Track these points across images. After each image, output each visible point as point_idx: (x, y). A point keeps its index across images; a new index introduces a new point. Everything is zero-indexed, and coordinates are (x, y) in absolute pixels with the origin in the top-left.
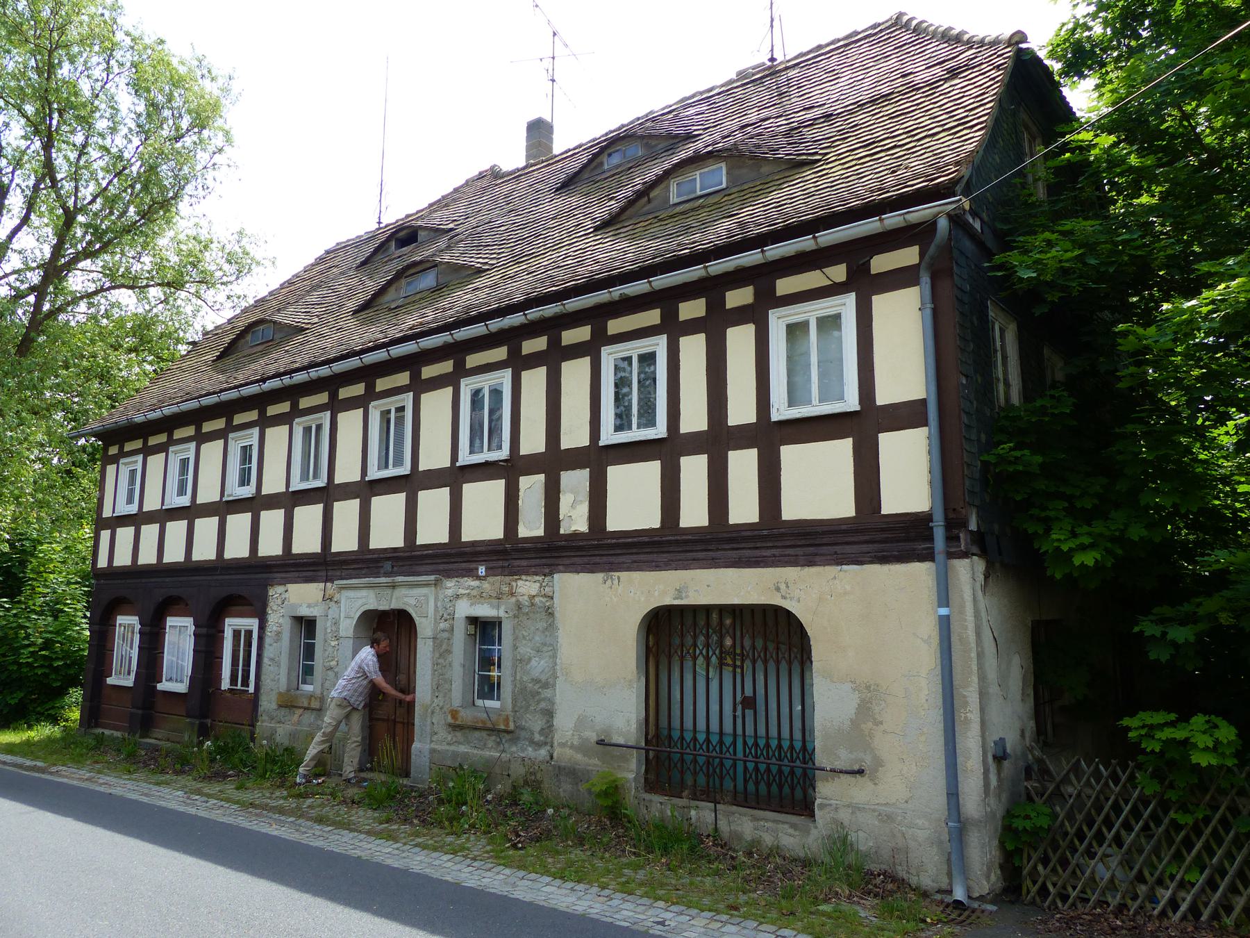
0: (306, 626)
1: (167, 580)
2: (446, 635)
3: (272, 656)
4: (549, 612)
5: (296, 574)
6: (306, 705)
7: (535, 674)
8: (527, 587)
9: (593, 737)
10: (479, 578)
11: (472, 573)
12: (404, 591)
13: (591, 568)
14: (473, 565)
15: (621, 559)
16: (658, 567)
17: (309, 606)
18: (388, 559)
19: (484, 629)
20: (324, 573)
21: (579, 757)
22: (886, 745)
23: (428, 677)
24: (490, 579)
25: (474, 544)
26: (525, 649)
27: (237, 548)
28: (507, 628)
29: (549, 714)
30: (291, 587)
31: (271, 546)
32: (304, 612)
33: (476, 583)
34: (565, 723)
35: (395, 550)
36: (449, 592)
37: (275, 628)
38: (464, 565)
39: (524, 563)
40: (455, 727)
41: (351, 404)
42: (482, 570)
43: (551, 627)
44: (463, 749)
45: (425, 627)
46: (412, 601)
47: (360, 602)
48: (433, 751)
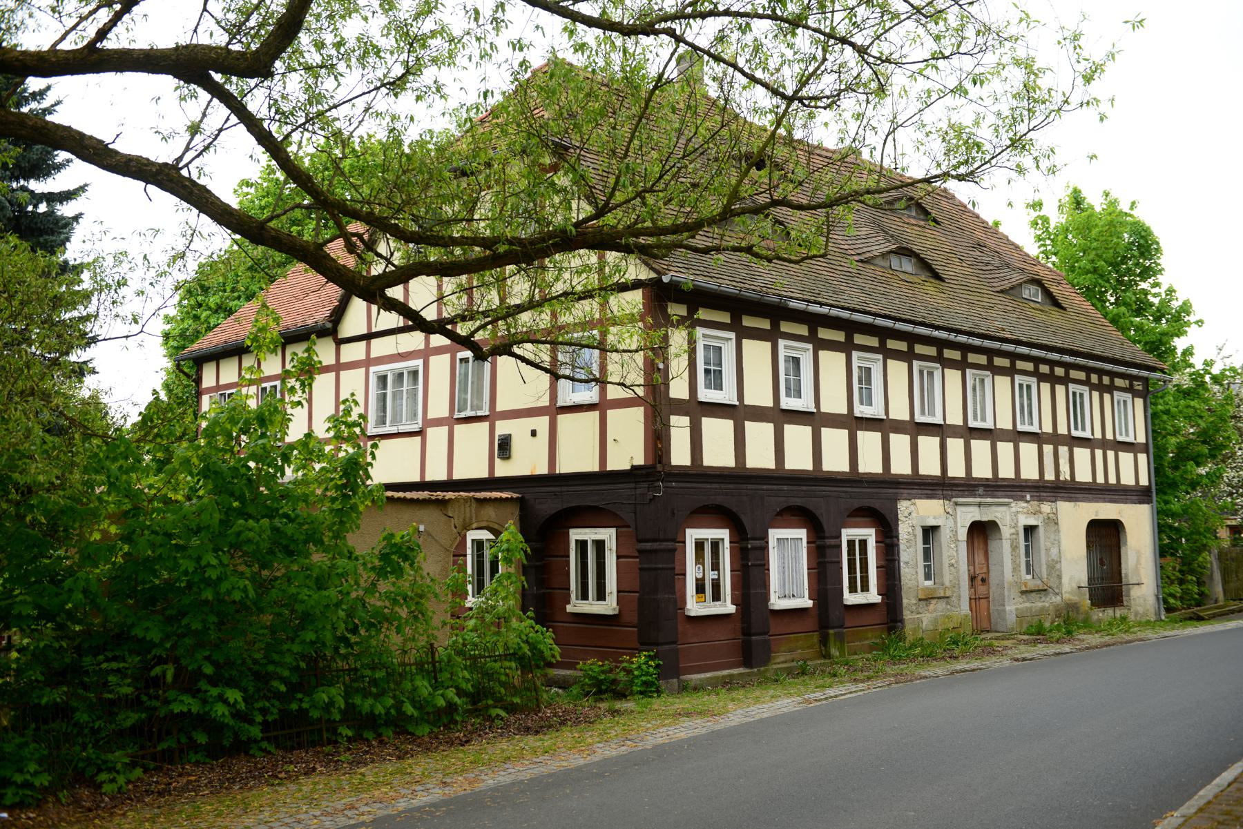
0: (929, 532)
1: (785, 488)
2: (1014, 536)
3: (906, 560)
4: (1057, 524)
5: (920, 491)
6: (942, 595)
7: (1053, 556)
8: (1046, 508)
9: (1075, 586)
10: (1027, 502)
11: (1022, 499)
12: (994, 508)
13: (1070, 500)
14: (1024, 494)
15: (1078, 495)
16: (1090, 501)
17: (935, 518)
18: (983, 485)
19: (1030, 530)
20: (940, 492)
21: (1072, 597)
22: (1142, 572)
23: (1010, 565)
24: (1032, 503)
25: (1026, 481)
26: (1049, 544)
27: (870, 463)
28: (1041, 530)
29: (1060, 577)
30: (918, 502)
31: (901, 466)
32: (931, 522)
33: (1025, 505)
34: (1065, 580)
35: (987, 479)
36: (1014, 510)
37: (907, 537)
38: (1019, 493)
39: (1044, 494)
40: (1023, 593)
41: (952, 364)
42: (1028, 497)
43: (1058, 531)
44: (1028, 605)
45: (1006, 531)
46: (999, 515)
47: (970, 515)
48: (1017, 609)
